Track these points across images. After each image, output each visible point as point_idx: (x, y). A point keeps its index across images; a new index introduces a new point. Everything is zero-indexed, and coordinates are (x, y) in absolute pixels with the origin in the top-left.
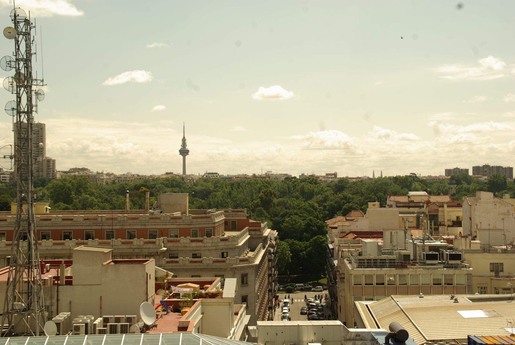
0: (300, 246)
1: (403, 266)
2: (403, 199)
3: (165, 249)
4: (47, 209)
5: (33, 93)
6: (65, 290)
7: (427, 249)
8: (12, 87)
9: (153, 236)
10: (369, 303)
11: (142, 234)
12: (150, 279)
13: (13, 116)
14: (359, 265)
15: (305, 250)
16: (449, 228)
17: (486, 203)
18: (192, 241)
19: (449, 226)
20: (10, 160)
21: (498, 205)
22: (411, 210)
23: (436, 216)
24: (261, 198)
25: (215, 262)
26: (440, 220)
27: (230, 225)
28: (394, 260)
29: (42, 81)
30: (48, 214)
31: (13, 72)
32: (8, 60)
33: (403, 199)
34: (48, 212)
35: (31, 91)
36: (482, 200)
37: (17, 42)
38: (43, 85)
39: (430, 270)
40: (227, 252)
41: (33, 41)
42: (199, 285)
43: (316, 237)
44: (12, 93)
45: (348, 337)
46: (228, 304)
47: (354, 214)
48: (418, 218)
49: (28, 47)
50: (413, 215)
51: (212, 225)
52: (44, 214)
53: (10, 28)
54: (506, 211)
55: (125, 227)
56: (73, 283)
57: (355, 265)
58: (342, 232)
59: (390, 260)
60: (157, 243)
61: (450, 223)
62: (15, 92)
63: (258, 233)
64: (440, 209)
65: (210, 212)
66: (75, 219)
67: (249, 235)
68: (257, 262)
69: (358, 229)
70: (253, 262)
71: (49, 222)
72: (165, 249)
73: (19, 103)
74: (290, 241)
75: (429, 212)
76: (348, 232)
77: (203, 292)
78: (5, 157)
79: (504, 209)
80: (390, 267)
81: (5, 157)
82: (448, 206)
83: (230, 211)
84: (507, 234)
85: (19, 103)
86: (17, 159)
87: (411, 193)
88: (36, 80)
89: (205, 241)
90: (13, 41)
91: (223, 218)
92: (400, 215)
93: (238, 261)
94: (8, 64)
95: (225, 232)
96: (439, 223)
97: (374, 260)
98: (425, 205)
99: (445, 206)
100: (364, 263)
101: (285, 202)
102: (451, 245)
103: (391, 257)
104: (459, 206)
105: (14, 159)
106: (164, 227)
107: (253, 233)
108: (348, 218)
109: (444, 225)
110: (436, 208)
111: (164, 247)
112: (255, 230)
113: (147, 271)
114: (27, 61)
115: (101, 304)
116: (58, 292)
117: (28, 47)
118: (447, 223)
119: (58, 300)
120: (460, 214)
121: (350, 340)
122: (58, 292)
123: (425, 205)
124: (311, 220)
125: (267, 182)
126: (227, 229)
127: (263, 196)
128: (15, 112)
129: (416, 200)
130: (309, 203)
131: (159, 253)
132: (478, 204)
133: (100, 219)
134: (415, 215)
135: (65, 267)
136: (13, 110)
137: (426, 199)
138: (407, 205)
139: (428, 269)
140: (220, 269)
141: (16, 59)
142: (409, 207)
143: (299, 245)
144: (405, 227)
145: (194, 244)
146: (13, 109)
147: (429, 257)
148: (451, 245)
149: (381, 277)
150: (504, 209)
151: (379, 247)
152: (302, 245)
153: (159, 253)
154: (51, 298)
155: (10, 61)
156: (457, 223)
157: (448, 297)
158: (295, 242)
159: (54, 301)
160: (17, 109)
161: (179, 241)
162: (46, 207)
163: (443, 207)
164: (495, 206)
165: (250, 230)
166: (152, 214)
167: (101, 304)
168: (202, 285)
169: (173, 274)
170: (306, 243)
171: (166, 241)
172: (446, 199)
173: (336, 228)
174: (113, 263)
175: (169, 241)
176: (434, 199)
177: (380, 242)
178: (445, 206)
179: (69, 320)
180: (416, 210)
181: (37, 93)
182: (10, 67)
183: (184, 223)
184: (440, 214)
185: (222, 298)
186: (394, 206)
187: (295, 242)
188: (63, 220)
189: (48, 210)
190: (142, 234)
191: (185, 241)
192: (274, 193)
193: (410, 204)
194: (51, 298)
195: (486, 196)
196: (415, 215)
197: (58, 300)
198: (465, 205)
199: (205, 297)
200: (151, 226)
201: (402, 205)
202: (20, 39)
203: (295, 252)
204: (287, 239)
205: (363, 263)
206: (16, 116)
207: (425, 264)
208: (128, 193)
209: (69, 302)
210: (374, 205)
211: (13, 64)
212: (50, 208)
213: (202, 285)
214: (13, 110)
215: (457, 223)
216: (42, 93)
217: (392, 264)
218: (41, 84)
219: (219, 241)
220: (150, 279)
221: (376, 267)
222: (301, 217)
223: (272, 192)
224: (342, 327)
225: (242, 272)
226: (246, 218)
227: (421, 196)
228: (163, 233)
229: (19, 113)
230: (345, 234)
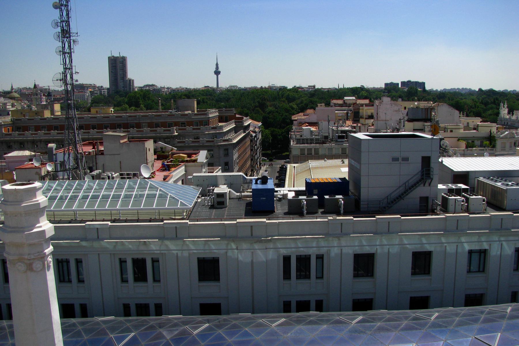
0: (279, 132)
1: (324, 143)
2: (340, 102)
3: (177, 134)
4: (111, 111)
5: (72, 41)
6: (100, 158)
7: (340, 132)
8: (59, 38)
9: (170, 125)
10: (295, 165)
11: (164, 125)
12: (149, 151)
13: (61, 55)
14: (297, 143)
15: (281, 135)
16: (366, 120)
17: (386, 104)
18: (194, 129)
19: (366, 119)
20: (60, 82)
21: (393, 105)
22: (344, 108)
23: (358, 112)
24: (258, 102)
25: (208, 141)
26: (361, 114)
27: (222, 119)
28: (319, 139)
29: (77, 33)
30: (113, 114)
31: (59, 30)
32: (56, 22)
33: (340, 102)
34: (112, 112)
35: (70, 40)
36: (384, 102)
37: (61, 10)
38: (77, 36)
39: (339, 145)
40: (216, 136)
41: (70, 9)
42: (186, 155)
43: (288, 126)
44: (59, 42)
45: (245, 182)
46: (201, 166)
47: (309, 111)
48: (347, 113)
49: (68, 15)
50: (344, 112)
51: (207, 119)
52: (111, 114)
53: (56, 2)
54: (398, 109)
55: (153, 121)
56: (104, 153)
57: (295, 143)
58: (300, 123)
59: (316, 139)
60: (172, 130)
61: (367, 117)
62: (61, 41)
63: (240, 124)
64: (361, 108)
65: (209, 111)
66: (123, 117)
67: (235, 125)
68: (235, 141)
69: (310, 121)
70: (232, 141)
71: (108, 119)
72: (177, 134)
73: (64, 48)
74: (272, 129)
75: (354, 110)
76: (304, 123)
77: (189, 159)
78: (57, 80)
79: (396, 108)
80: (316, 143)
81: (57, 80)
82: (366, 106)
83: (224, 110)
84: (387, 122)
85: (64, 48)
86: (64, 81)
87: (346, 98)
88: (72, 33)
89: (201, 129)
90: (58, 10)
91: (217, 114)
92: (336, 112)
93: (222, 141)
94: (56, 24)
95: (219, 123)
96: (360, 117)
97: (306, 139)
98: (352, 106)
99: (364, 106)
100: (300, 141)
101: (275, 104)
102: (355, 130)
103: (317, 137)
104: (373, 106)
105: (62, 81)
106: (177, 120)
107: (237, 124)
108: (305, 114)
109: (363, 118)
110: (358, 107)
111: (176, 133)
112: (238, 122)
113: (146, 146)
114: (68, 22)
115: (120, 166)
116: (96, 159)
117: (68, 15)
118: (364, 117)
119: (96, 163)
120: (373, 111)
121: (247, 183)
122: (96, 159)
123: (352, 106)
124: (286, 116)
125: (264, 92)
126: (220, 122)
127: (260, 101)
128: (61, 53)
129: (348, 102)
130: (289, 105)
131: (173, 137)
132: (381, 105)
133: (138, 117)
134: (346, 111)
135: (99, 145)
136: (60, 52)
137: (354, 102)
138: (341, 105)
139: (339, 144)
140: (211, 146)
141: (61, 21)
142: (342, 106)
143: (277, 132)
144: (328, 119)
145: (195, 131)
146: (60, 51)
147: (340, 137)
148: (355, 130)
149: (310, 150)
150: (396, 108)
151: (312, 132)
152: (280, 131)
153: (173, 137)
154: (93, 163)
155: (57, 23)
156: (371, 117)
157: (340, 160)
158: (275, 129)
159: (95, 164)
160: (63, 51)
161: (185, 129)
162: (111, 109)
163: (363, 106)
164: (391, 106)
165: (235, 122)
166: (171, 112)
167: (120, 166)
168: (189, 156)
169: (176, 149)
170: (282, 130)
171: (177, 130)
172: (367, 101)
173: (296, 120)
174: (128, 142)
175: (179, 129)
176: (360, 102)
177: (313, 129)
178: (364, 106)
179: (100, 174)
180: (346, 108)
181: (74, 41)
182: (57, 26)
183: (189, 118)
184: (361, 111)
185: (197, 162)
186: (333, 106)
187: (275, 129)
188: (116, 117)
189: (112, 111)
190: (164, 125)
191: (189, 128)
192: (267, 98)
193: (345, 104)
194: (93, 163)
195: (386, 100)
196: (346, 111)
197: (96, 163)
198: (375, 106)
199: (190, 162)
200: (169, 120)
201: (338, 105)
202: (63, 9)
203: (274, 136)
204: (270, 128)
205: (299, 141)
206: (62, 56)
207: (336, 141)
208: (160, 100)
209: (102, 165)
210: (321, 106)
211: (59, 24)
212: (113, 110)
213: (189, 156)
214: (60, 52)
215: (371, 117)
216: (77, 41)
217: (318, 142)
218: (76, 35)
219: (211, 128)
220: (149, 151)
221: (307, 143)
222: (280, 113)
223: (266, 98)
224: (242, 176)
225: (225, 148)
226: (234, 114)
227: (350, 100)
228: (176, 124)
229: (64, 53)
230: (302, 124)
